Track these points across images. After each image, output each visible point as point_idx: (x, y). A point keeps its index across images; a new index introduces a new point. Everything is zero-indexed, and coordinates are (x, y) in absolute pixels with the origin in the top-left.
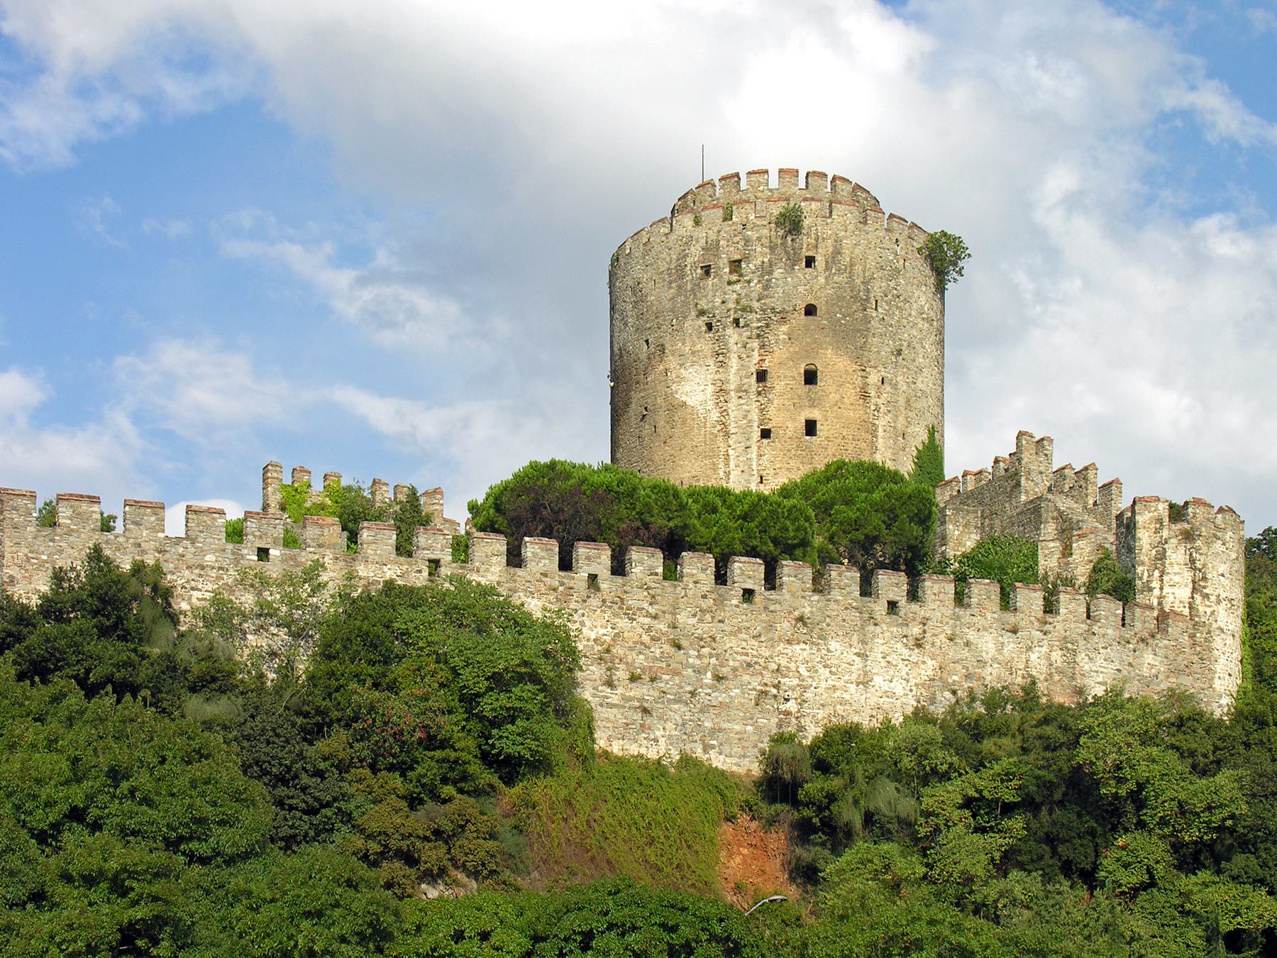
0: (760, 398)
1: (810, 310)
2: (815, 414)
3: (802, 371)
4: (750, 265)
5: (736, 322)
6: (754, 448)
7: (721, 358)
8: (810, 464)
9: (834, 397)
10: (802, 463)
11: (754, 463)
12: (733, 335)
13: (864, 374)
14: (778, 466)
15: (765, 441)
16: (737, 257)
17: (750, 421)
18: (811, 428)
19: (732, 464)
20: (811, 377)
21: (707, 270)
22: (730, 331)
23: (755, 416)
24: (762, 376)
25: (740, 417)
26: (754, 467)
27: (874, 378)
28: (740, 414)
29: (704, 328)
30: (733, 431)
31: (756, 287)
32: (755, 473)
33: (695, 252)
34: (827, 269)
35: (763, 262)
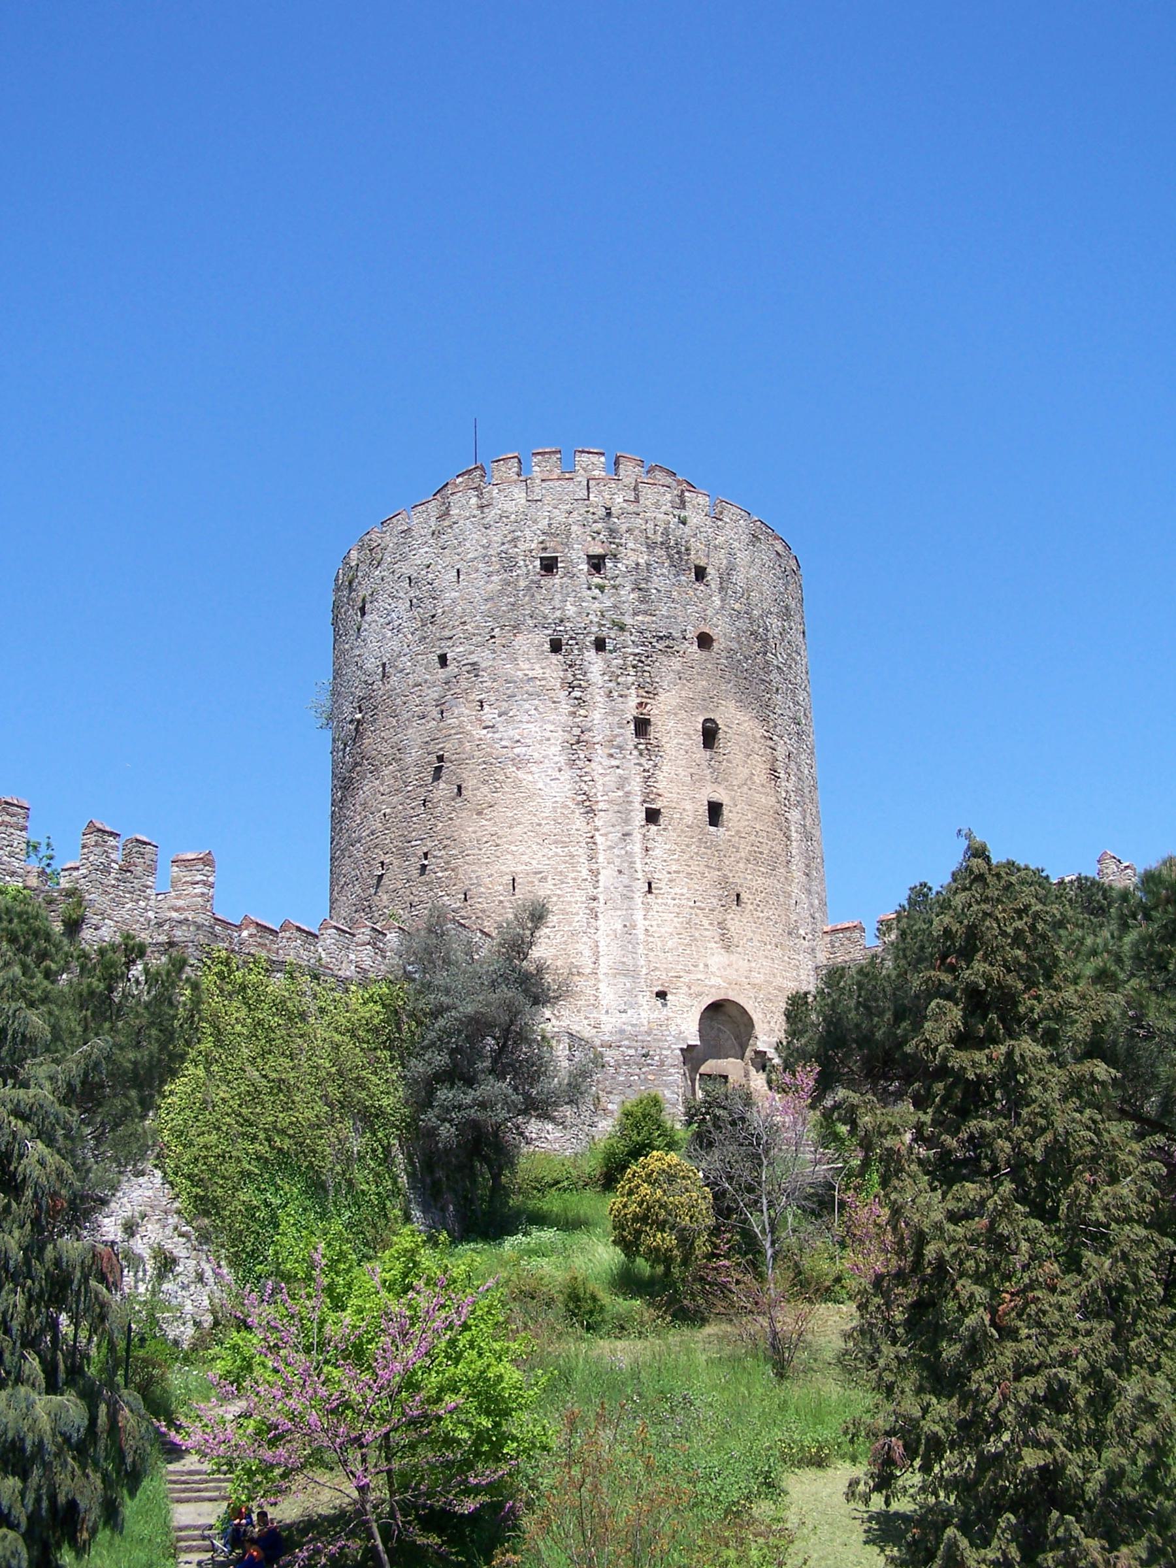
0: (643, 761)
1: (705, 641)
2: (721, 796)
3: (700, 727)
4: (619, 565)
5: (600, 645)
6: (637, 836)
7: (577, 694)
8: (719, 870)
9: (743, 772)
10: (707, 866)
11: (638, 860)
12: (595, 663)
13: (771, 743)
14: (674, 868)
15: (653, 828)
16: (599, 550)
17: (628, 794)
18: (715, 811)
19: (601, 858)
20: (710, 735)
21: (549, 566)
22: (591, 654)
23: (636, 785)
24: (642, 726)
25: (613, 786)
26: (638, 866)
27: (781, 752)
28: (611, 780)
29: (547, 647)
30: (601, 806)
31: (628, 596)
32: (640, 875)
33: (530, 541)
34: (721, 589)
35: (638, 564)
